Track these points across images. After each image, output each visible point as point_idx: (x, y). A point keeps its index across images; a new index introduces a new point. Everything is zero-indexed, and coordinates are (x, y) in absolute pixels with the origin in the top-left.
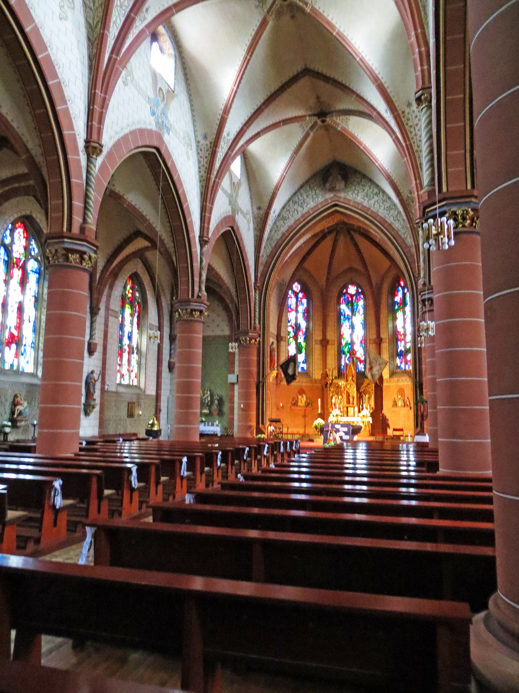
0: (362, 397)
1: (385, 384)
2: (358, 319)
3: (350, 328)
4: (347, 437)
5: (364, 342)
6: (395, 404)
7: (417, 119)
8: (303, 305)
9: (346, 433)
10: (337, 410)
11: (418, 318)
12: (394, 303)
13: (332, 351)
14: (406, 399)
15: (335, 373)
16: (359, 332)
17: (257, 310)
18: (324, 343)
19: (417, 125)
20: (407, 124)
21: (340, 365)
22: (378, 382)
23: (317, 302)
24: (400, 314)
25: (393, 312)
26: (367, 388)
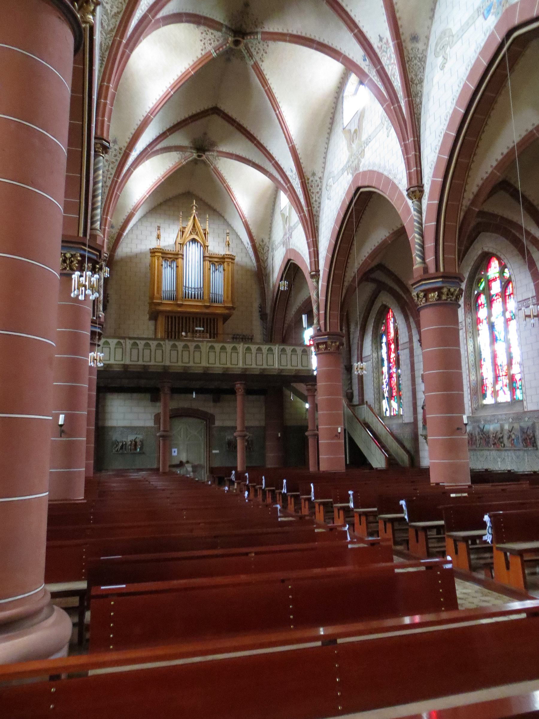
7: (318, 188)
19: (318, 193)
20: (310, 190)
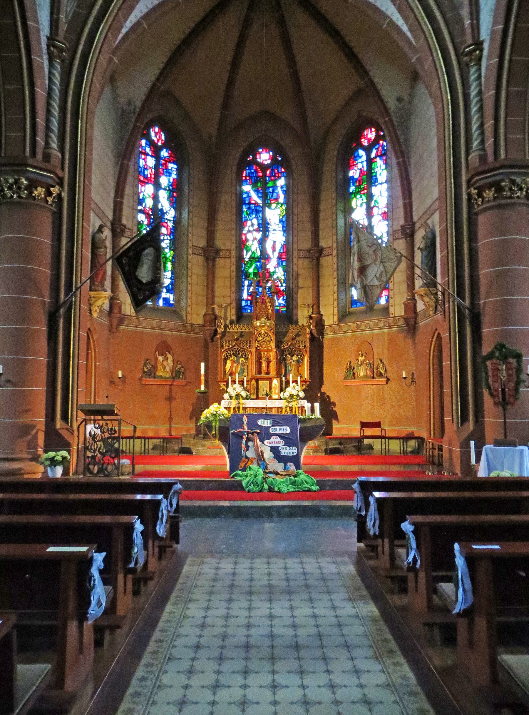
0: (285, 359)
1: (328, 335)
2: (274, 214)
3: (257, 230)
4: (292, 451)
5: (286, 256)
6: (351, 373)
8: (170, 174)
9: (288, 440)
10: (237, 385)
11: (468, 154)
12: (348, 180)
13: (225, 269)
14: (377, 362)
15: (232, 314)
16: (277, 237)
17: (56, 111)
18: (211, 254)
21: (240, 299)
22: (314, 332)
23: (197, 173)
24: (358, 204)
25: (345, 197)
26: (294, 341)
